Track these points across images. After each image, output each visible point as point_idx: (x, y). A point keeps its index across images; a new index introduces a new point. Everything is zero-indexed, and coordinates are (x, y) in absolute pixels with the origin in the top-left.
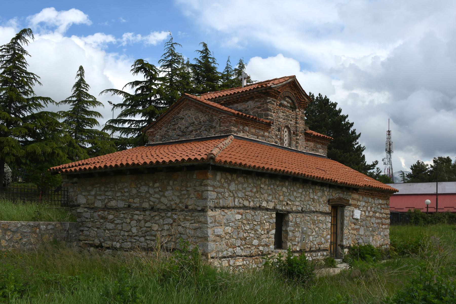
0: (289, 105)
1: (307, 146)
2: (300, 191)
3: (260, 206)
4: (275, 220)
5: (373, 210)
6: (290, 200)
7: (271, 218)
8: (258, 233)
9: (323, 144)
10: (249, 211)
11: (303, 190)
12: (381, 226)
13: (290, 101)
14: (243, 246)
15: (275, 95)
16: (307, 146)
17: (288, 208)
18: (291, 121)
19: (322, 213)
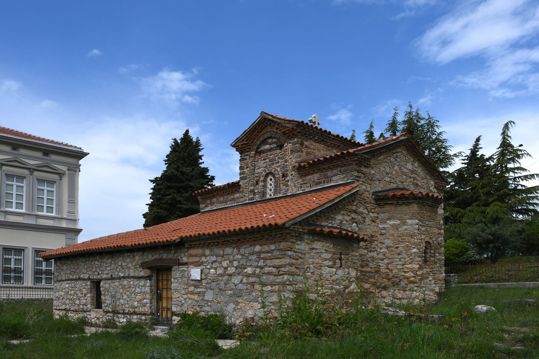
0: (273, 146)
1: (304, 183)
2: (109, 261)
3: (79, 278)
4: (89, 287)
5: (235, 263)
6: (101, 271)
7: (87, 285)
8: (78, 296)
9: (341, 167)
10: (73, 282)
11: (112, 260)
12: (257, 287)
13: (274, 140)
14: (71, 304)
15: (244, 149)
16: (304, 183)
17: (99, 277)
18: (278, 162)
19: (134, 277)
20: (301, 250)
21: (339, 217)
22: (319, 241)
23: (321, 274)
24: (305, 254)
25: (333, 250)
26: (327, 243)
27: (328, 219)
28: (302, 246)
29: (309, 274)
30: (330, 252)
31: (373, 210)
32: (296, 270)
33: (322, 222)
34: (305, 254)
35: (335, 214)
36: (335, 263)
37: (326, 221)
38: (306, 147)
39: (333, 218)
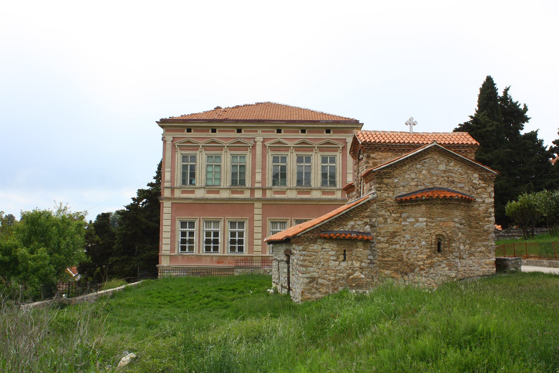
20: (314, 250)
21: (352, 223)
22: (327, 243)
23: (329, 266)
24: (317, 252)
25: (336, 249)
26: (332, 244)
27: (339, 225)
28: (316, 247)
29: (320, 266)
30: (335, 250)
31: (396, 212)
32: (309, 264)
33: (334, 229)
34: (317, 252)
35: (347, 221)
36: (338, 258)
37: (337, 227)
38: (373, 158)
39: (345, 224)
